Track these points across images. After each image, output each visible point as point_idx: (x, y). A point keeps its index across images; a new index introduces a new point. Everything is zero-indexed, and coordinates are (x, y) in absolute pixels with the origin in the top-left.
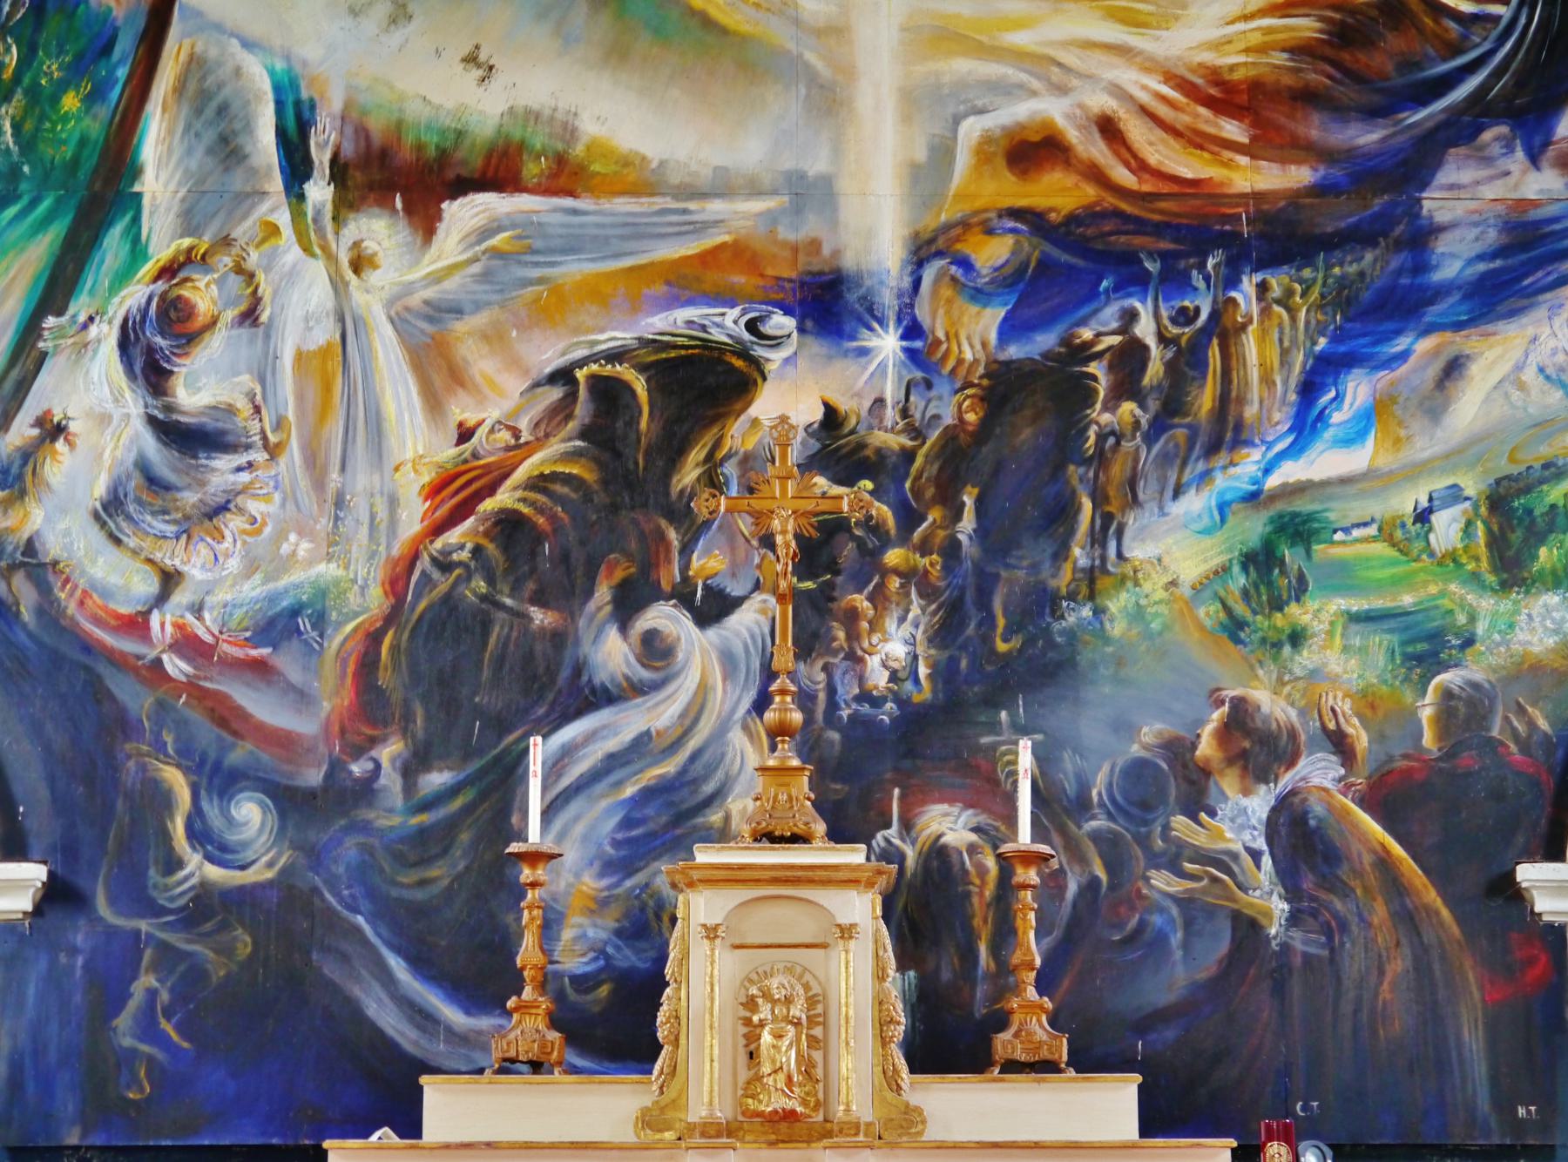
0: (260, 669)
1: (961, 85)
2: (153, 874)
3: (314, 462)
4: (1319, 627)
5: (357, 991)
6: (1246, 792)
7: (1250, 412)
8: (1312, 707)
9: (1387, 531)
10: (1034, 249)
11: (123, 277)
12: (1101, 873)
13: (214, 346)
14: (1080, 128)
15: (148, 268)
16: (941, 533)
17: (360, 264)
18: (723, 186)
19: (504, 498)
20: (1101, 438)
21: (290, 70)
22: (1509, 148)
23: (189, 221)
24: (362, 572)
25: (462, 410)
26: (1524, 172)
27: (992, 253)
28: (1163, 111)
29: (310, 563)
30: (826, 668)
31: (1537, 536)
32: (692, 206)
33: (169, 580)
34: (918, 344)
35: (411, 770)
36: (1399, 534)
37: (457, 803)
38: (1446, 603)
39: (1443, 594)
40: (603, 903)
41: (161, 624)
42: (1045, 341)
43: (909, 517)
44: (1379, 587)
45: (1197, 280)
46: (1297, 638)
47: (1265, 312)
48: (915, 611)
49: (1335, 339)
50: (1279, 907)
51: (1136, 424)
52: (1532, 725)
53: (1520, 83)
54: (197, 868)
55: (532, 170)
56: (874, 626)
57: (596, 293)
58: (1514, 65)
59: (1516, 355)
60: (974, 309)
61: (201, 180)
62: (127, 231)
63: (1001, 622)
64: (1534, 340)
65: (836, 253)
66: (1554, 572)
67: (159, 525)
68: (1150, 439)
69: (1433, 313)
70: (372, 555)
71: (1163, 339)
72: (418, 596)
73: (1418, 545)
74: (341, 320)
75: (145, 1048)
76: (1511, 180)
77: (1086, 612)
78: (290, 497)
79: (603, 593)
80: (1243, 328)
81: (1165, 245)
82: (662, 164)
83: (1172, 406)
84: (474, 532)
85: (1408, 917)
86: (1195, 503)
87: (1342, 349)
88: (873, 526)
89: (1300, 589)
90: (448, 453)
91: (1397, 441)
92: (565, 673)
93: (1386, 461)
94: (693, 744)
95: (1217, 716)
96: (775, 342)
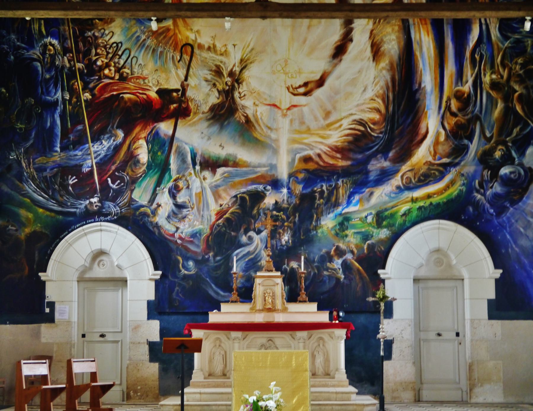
0: (191, 242)
1: (297, 149)
2: (177, 273)
3: (199, 210)
4: (350, 234)
5: (207, 289)
6: (338, 259)
7: (340, 201)
8: (348, 246)
9: (361, 219)
10: (308, 175)
11: (169, 181)
12: (316, 271)
13: (183, 192)
14: (315, 156)
15: (172, 180)
16: (293, 220)
17: (204, 179)
18: (260, 166)
19: (227, 215)
20: (317, 205)
21: (192, 148)
22: (382, 158)
23: (178, 172)
24: (206, 227)
25: (220, 202)
27: (301, 176)
28: (328, 153)
29: (198, 225)
30: (276, 241)
31: (384, 219)
32: (255, 169)
33: (178, 228)
34: (290, 191)
35: (215, 256)
36: (362, 220)
37: (221, 262)
38: (369, 230)
39: (369, 229)
40: (242, 277)
41: (177, 235)
42: (309, 190)
43: (288, 218)
44: (359, 228)
45: (333, 180)
46: (346, 236)
47: (343, 185)
48: (289, 232)
49: (354, 189)
50: (343, 276)
51: (323, 203)
52: (381, 249)
54: (184, 272)
55: (231, 163)
56: (283, 234)
57: (241, 183)
59: (381, 191)
60: (298, 185)
61: (180, 166)
62: (169, 174)
63: (302, 234)
64: (384, 189)
65: (277, 176)
67: (176, 220)
68: (325, 205)
69: (369, 185)
70: (208, 224)
71: (327, 189)
72: (215, 231)
73: (365, 222)
74: (202, 188)
75: (177, 298)
76: (382, 163)
77: (315, 232)
78: (195, 216)
79: (242, 230)
80: (340, 187)
81: (328, 174)
82: (250, 162)
83: (328, 200)
84: (223, 221)
85: (362, 278)
86: (332, 215)
87: (355, 191)
88: (282, 219)
89: (347, 229)
90: (219, 208)
91: (363, 206)
92: (237, 242)
93: (361, 208)
94: (256, 253)
95: (334, 248)
96: (268, 191)
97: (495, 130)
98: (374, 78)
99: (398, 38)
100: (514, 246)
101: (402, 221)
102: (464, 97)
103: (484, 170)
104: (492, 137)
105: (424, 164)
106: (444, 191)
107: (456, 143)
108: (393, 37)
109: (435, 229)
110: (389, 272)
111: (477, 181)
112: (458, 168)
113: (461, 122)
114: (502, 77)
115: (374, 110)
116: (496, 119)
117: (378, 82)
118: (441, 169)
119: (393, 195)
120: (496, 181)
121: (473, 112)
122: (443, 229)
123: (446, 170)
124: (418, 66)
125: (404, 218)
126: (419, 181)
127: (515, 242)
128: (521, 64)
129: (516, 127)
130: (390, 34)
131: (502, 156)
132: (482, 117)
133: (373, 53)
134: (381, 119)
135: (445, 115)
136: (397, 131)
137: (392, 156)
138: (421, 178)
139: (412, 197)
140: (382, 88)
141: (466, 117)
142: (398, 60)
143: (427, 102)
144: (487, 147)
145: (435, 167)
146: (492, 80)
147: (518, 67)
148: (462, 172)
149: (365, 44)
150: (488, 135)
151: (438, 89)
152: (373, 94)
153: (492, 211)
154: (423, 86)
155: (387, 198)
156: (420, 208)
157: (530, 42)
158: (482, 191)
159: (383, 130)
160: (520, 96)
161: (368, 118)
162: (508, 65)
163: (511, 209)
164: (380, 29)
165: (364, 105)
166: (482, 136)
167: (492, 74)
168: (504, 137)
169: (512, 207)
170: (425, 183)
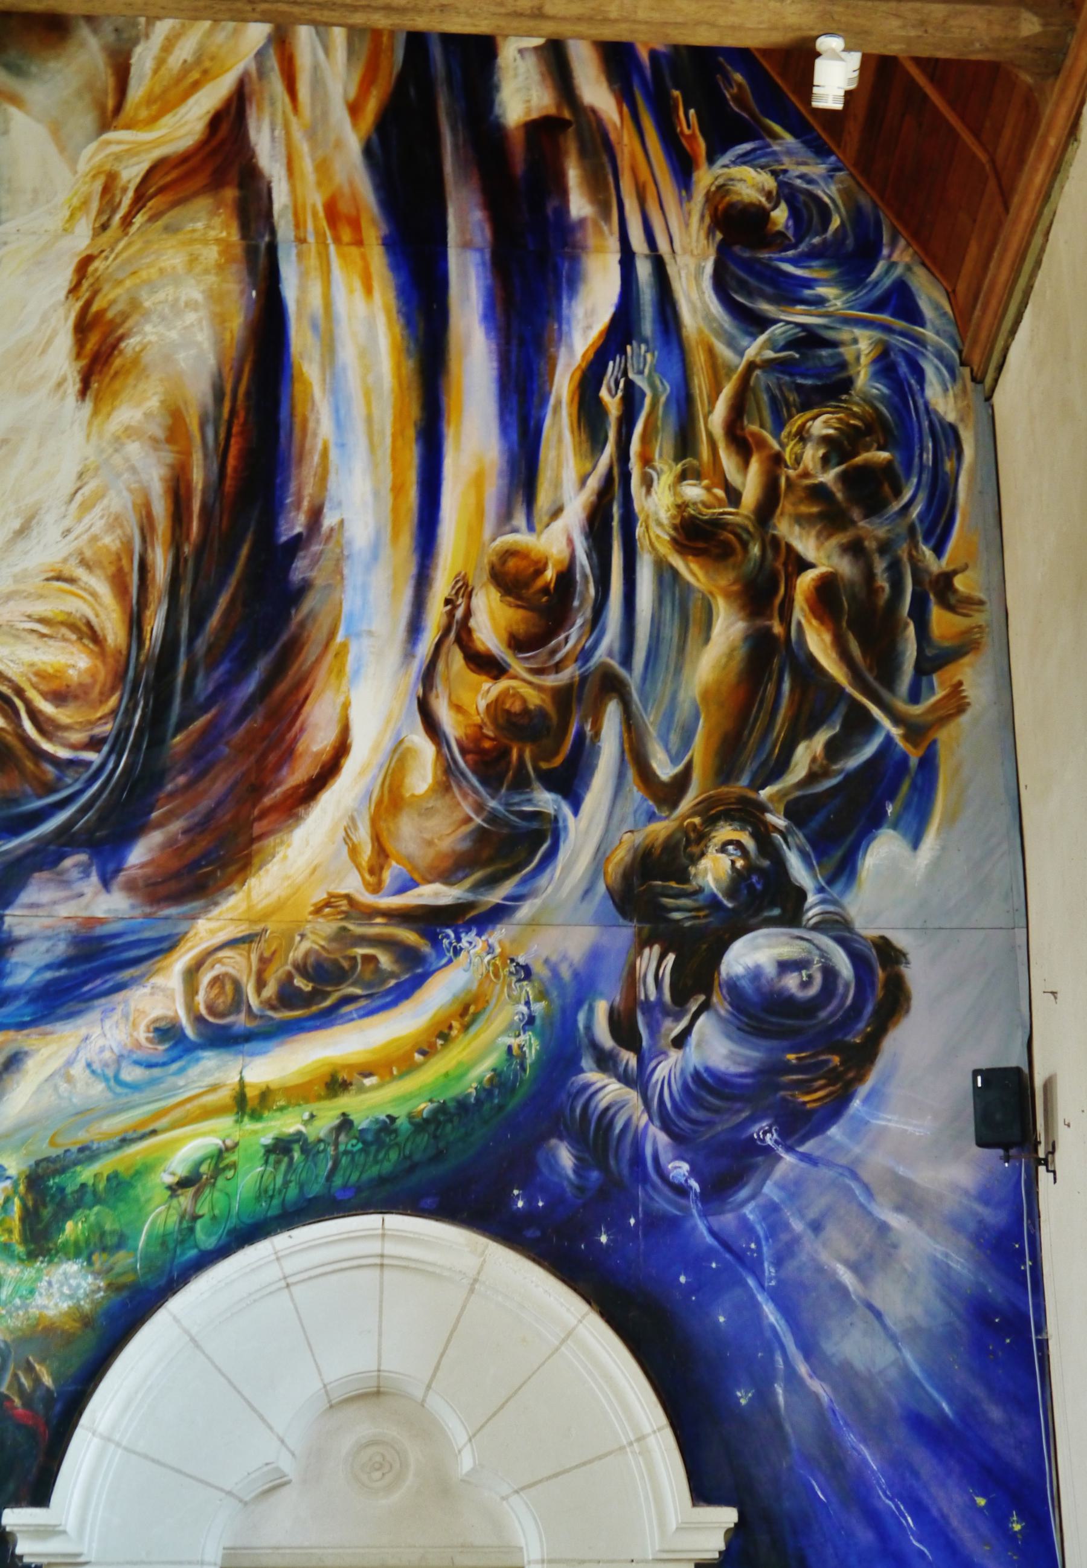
22: (86, 874)
26: (96, 894)
31: (66, 1210)
52: (37, 1381)
53: (102, 819)
58: (98, 804)
59: (68, 1051)
66: (76, 1243)
76: (83, 901)
97: (699, 751)
98: (80, 476)
99: (215, 297)
100: (803, 1369)
101: (174, 1219)
102: (540, 583)
103: (640, 953)
104: (682, 782)
105: (318, 910)
106: (418, 1057)
107: (492, 804)
108: (192, 291)
109: (357, 1264)
110: (70, 1524)
111: (602, 1008)
112: (499, 934)
113: (524, 701)
114: (734, 496)
115: (64, 631)
116: (706, 695)
117: (99, 496)
118: (409, 936)
119: (132, 1074)
120: (705, 1007)
121: (585, 655)
122: (407, 1266)
123: (435, 941)
124: (311, 425)
125: (185, 1199)
126: (287, 997)
127: (809, 1350)
128: (825, 440)
129: (809, 733)
130: (177, 281)
131: (738, 881)
132: (633, 679)
133: (84, 362)
134: (102, 675)
135: (441, 666)
136: (178, 738)
137: (143, 866)
138: (299, 982)
139: (242, 1083)
140: (115, 522)
141: (551, 681)
142: (209, 400)
143: (350, 600)
144: (661, 829)
145: (378, 928)
146: (682, 507)
147: (811, 455)
148: (521, 960)
149: (44, 319)
150: (664, 769)
151: (407, 539)
152: (64, 553)
153: (680, 1169)
154: (329, 520)
155: (99, 1087)
156: (281, 1147)
157: (864, 346)
158: (629, 1058)
159: (107, 728)
160: (827, 588)
161: (32, 665)
162: (762, 444)
163: (788, 1158)
164: (125, 255)
165: (11, 603)
166: (631, 774)
167: (683, 476)
168: (744, 781)
169: (790, 1149)
170: (314, 1009)
